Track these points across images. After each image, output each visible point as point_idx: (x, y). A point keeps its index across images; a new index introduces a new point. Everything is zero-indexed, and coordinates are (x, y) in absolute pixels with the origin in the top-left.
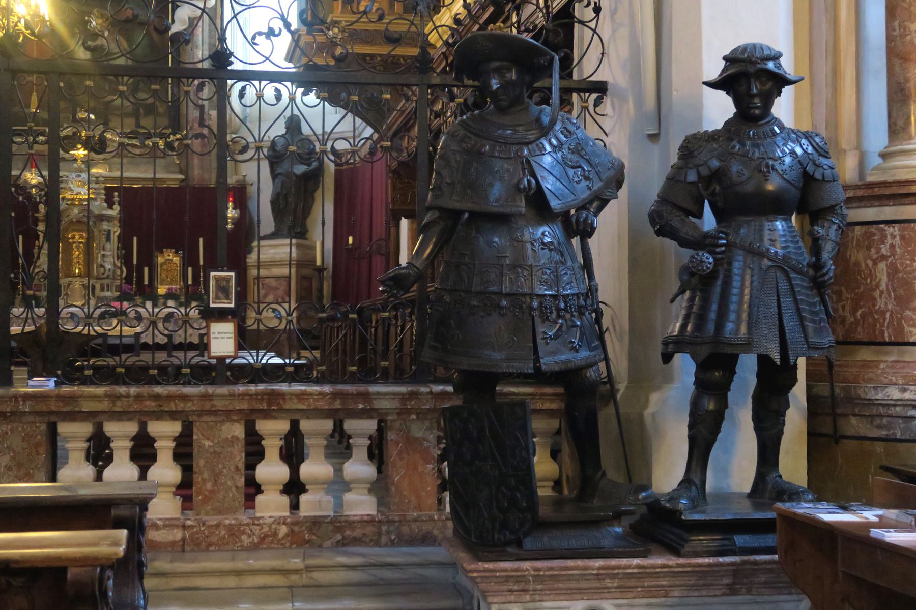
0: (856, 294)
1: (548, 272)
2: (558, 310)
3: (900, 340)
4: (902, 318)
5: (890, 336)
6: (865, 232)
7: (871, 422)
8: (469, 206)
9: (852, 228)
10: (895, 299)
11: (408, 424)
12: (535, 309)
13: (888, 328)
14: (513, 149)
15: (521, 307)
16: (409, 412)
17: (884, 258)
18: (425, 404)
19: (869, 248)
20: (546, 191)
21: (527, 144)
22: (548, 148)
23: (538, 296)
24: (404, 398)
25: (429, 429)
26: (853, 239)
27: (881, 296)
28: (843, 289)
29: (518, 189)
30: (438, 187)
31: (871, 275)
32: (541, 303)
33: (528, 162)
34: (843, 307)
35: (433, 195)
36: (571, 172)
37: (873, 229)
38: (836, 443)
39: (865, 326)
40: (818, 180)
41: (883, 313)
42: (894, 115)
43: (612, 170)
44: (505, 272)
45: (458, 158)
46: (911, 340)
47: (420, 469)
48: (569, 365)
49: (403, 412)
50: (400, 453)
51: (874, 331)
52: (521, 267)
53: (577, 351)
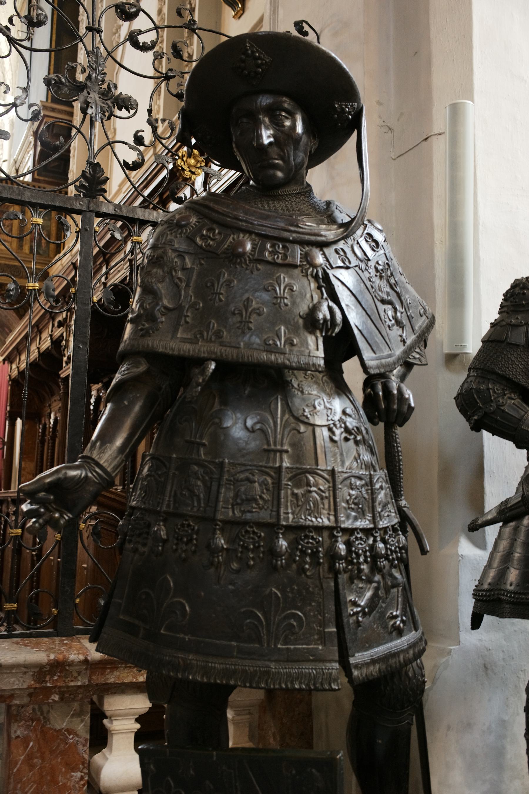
1: (358, 483)
2: (375, 556)
8: (217, 349)
11: (45, 708)
12: (341, 558)
14: (298, 251)
15: (315, 554)
16: (47, 692)
18: (76, 679)
20: (356, 331)
21: (323, 245)
22: (354, 262)
23: (345, 531)
24: (41, 671)
25: (79, 714)
29: (311, 322)
30: (147, 317)
32: (348, 544)
33: (326, 277)
35: (134, 332)
36: (381, 307)
43: (424, 317)
44: (284, 482)
45: (189, 263)
47: (61, 780)
48: (392, 661)
49: (39, 694)
50: (30, 757)
52: (313, 473)
53: (400, 633)
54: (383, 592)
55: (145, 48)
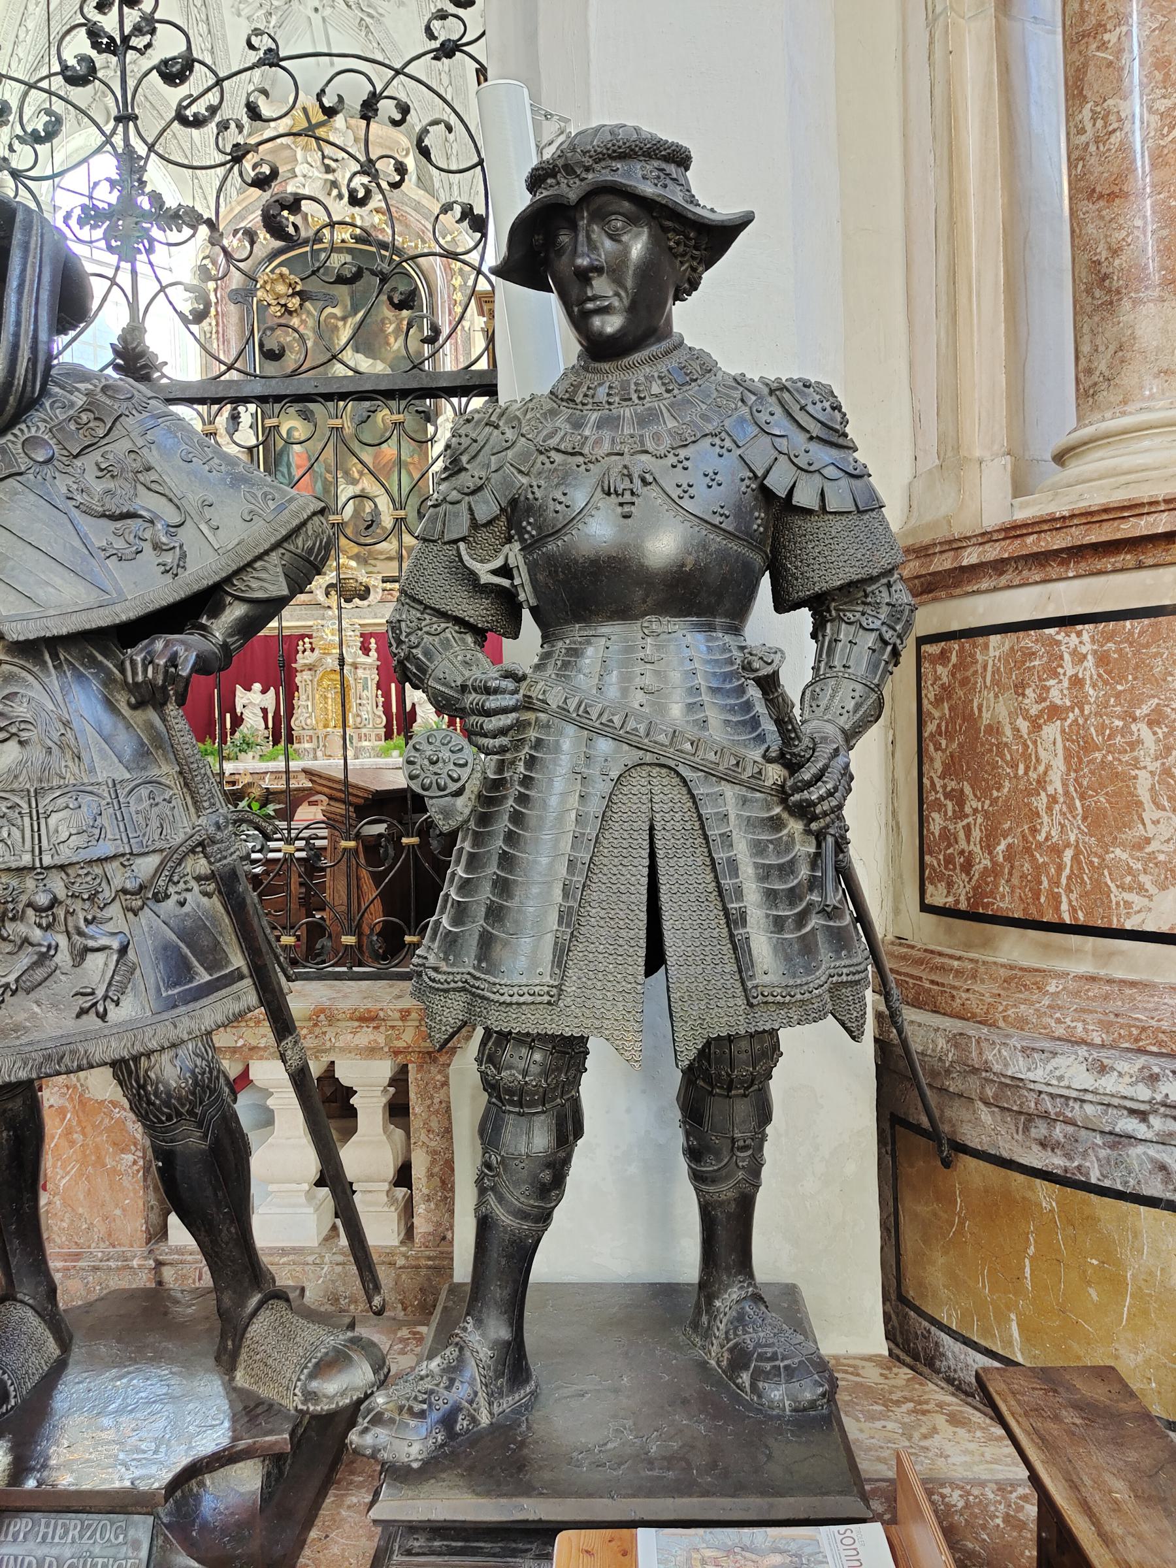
0: (994, 802)
3: (1099, 923)
4: (1103, 865)
5: (1073, 910)
6: (1012, 648)
7: (1026, 1129)
9: (981, 640)
10: (1084, 819)
13: (1069, 890)
17: (1055, 712)
19: (1020, 688)
26: (985, 667)
27: (1049, 809)
28: (968, 790)
31: (1026, 757)
34: (968, 829)
37: (1028, 640)
38: (947, 1164)
39: (1015, 881)
40: (808, 512)
41: (1056, 851)
42: (1086, 349)
46: (1128, 927)
51: (1037, 895)
54: (68, 958)
55: (198, 122)
